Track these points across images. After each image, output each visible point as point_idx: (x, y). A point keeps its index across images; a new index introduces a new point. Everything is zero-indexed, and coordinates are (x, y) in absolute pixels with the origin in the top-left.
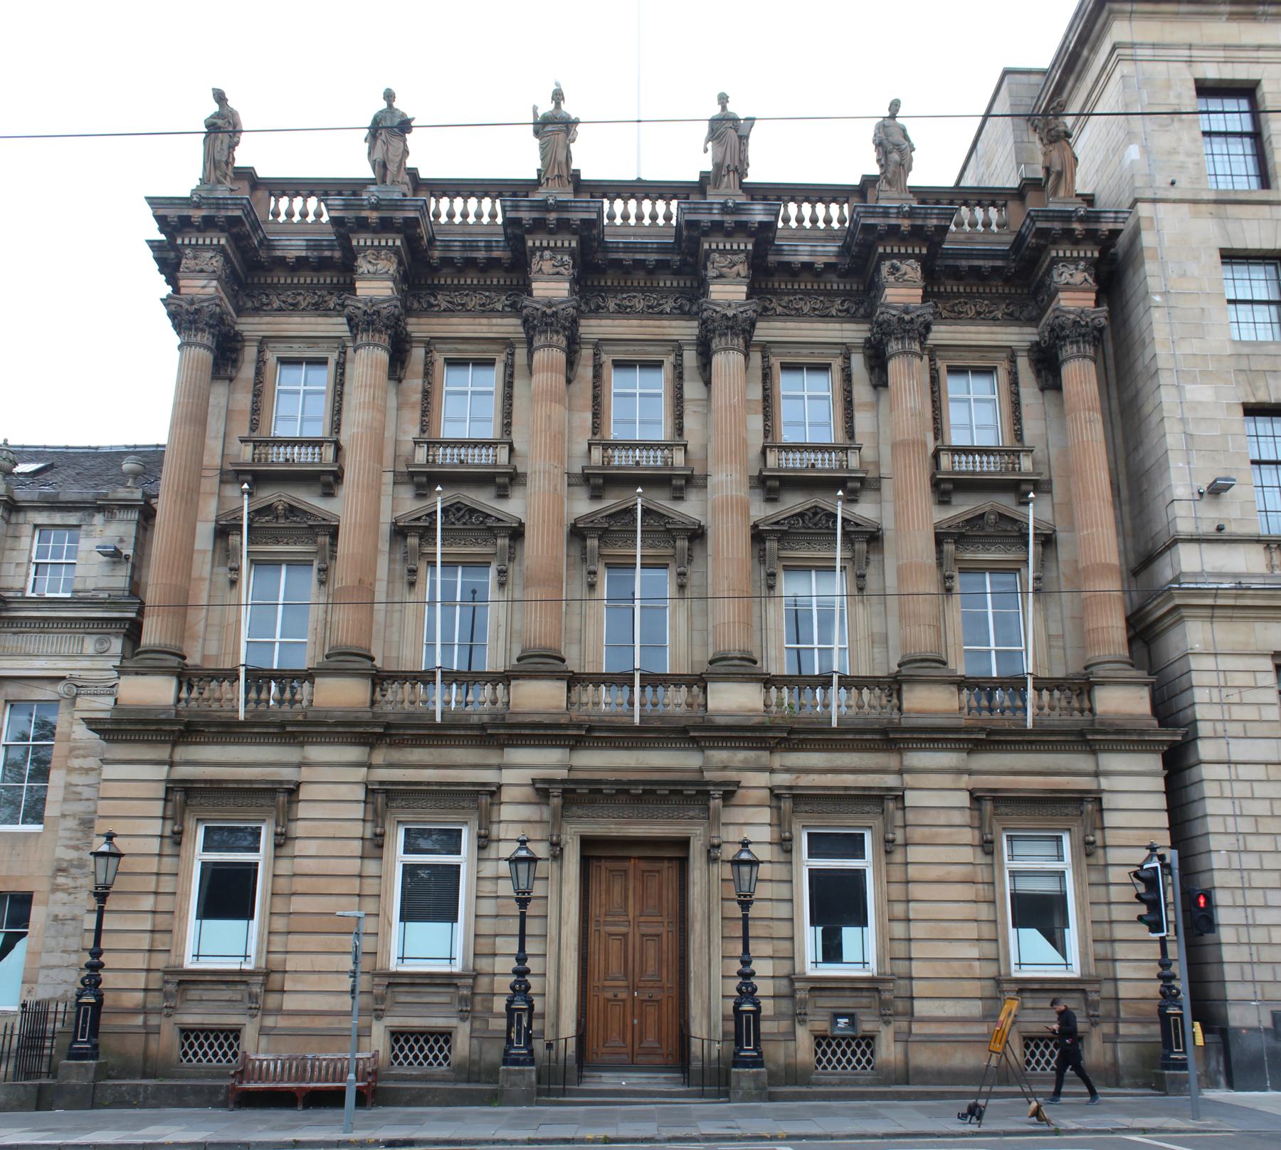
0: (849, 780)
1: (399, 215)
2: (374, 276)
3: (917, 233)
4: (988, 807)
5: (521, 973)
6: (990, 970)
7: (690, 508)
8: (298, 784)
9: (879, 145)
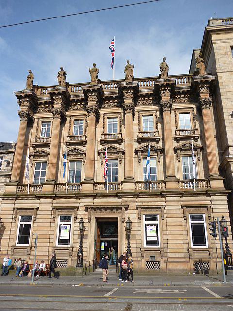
0: (154, 204)
1: (61, 91)
2: (57, 104)
3: (168, 85)
4: (185, 208)
5: (81, 247)
6: (186, 246)
7: (122, 147)
8: (38, 207)
9: (161, 67)
